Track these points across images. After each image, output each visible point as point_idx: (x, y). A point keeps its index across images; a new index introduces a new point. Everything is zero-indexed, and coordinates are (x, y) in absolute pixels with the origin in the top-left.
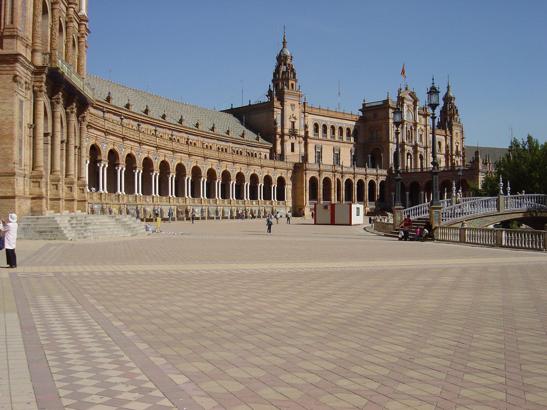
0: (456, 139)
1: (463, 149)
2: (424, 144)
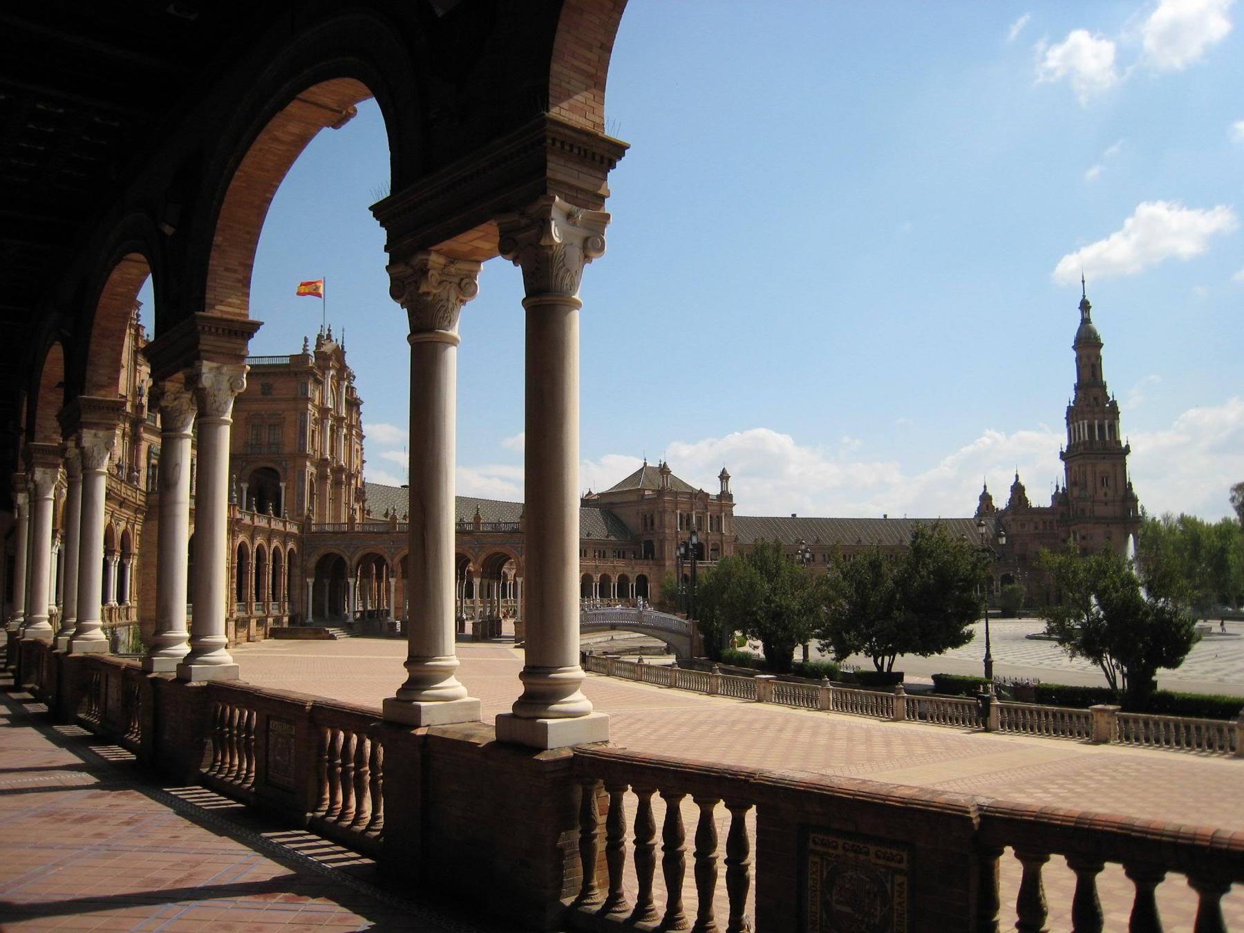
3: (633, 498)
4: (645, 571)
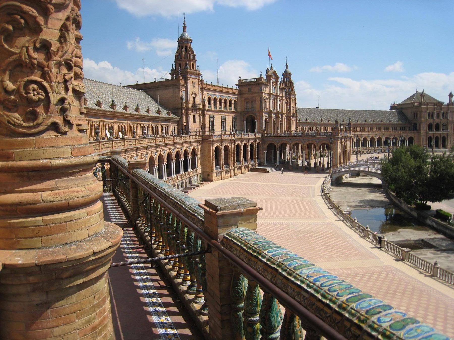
0: (293, 104)
1: (296, 111)
2: (281, 111)
3: (410, 106)
4: (413, 135)
